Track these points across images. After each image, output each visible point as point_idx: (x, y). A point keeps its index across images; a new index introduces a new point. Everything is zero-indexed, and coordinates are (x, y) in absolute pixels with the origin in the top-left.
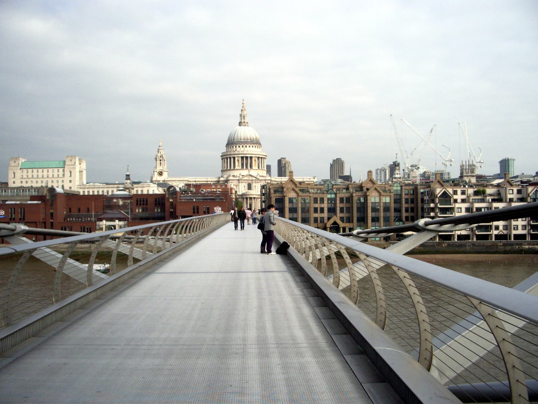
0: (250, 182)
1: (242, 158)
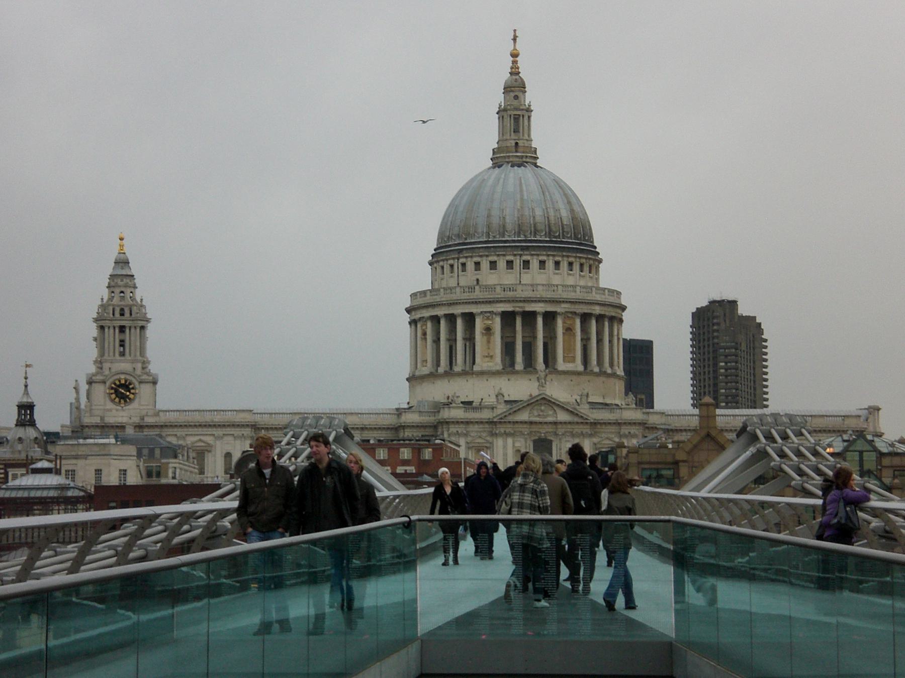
0: (544, 431)
1: (508, 318)
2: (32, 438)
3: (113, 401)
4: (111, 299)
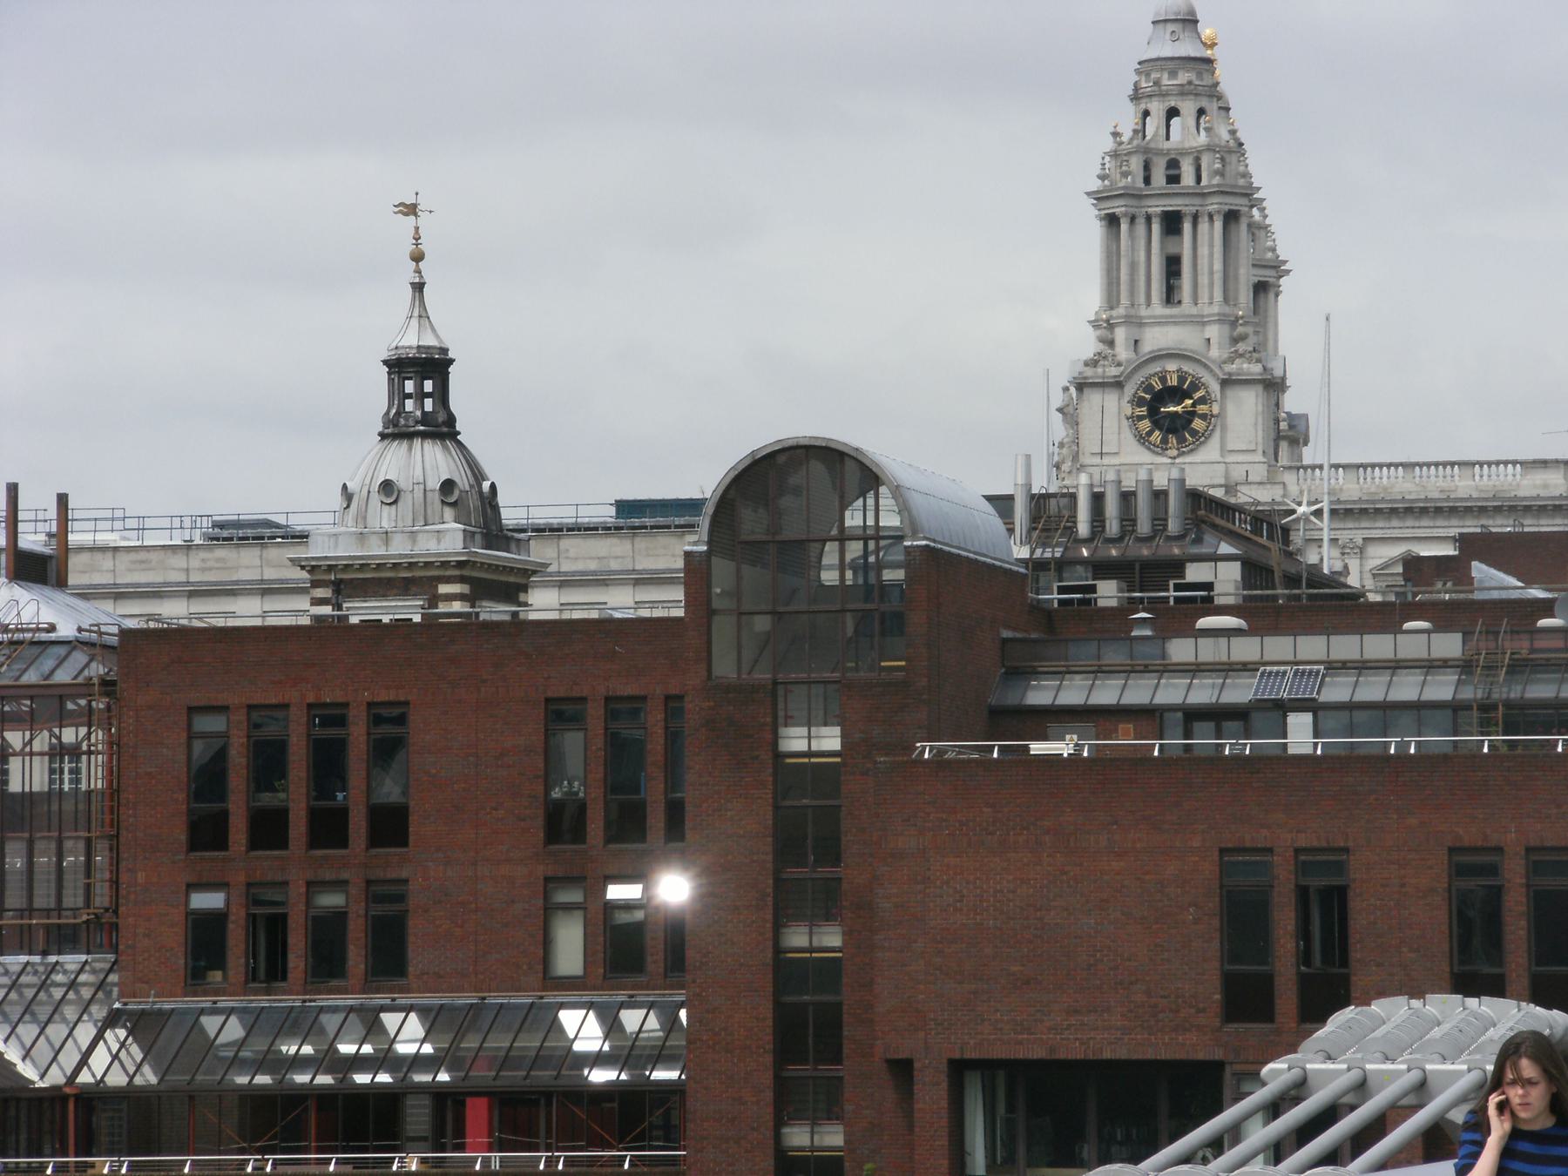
2: (434, 484)
3: (1143, 439)
4: (1141, 131)
